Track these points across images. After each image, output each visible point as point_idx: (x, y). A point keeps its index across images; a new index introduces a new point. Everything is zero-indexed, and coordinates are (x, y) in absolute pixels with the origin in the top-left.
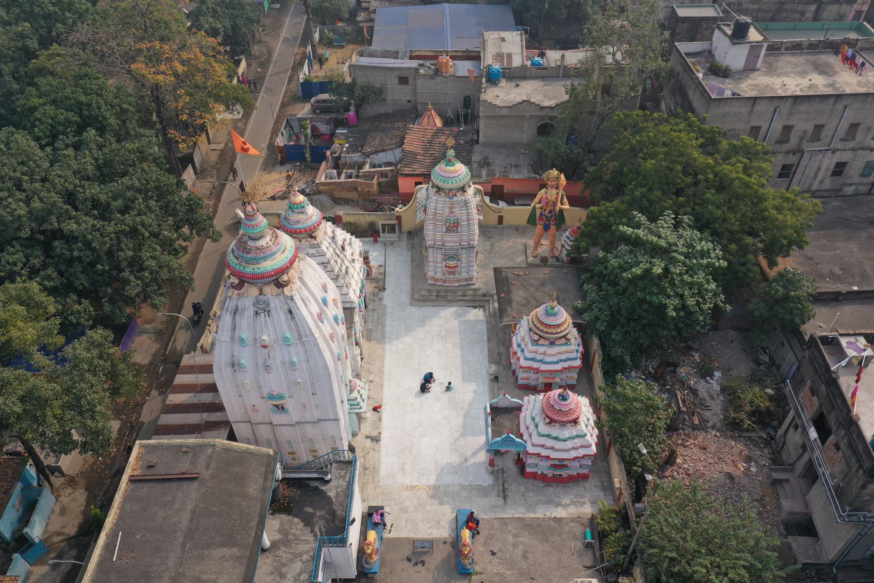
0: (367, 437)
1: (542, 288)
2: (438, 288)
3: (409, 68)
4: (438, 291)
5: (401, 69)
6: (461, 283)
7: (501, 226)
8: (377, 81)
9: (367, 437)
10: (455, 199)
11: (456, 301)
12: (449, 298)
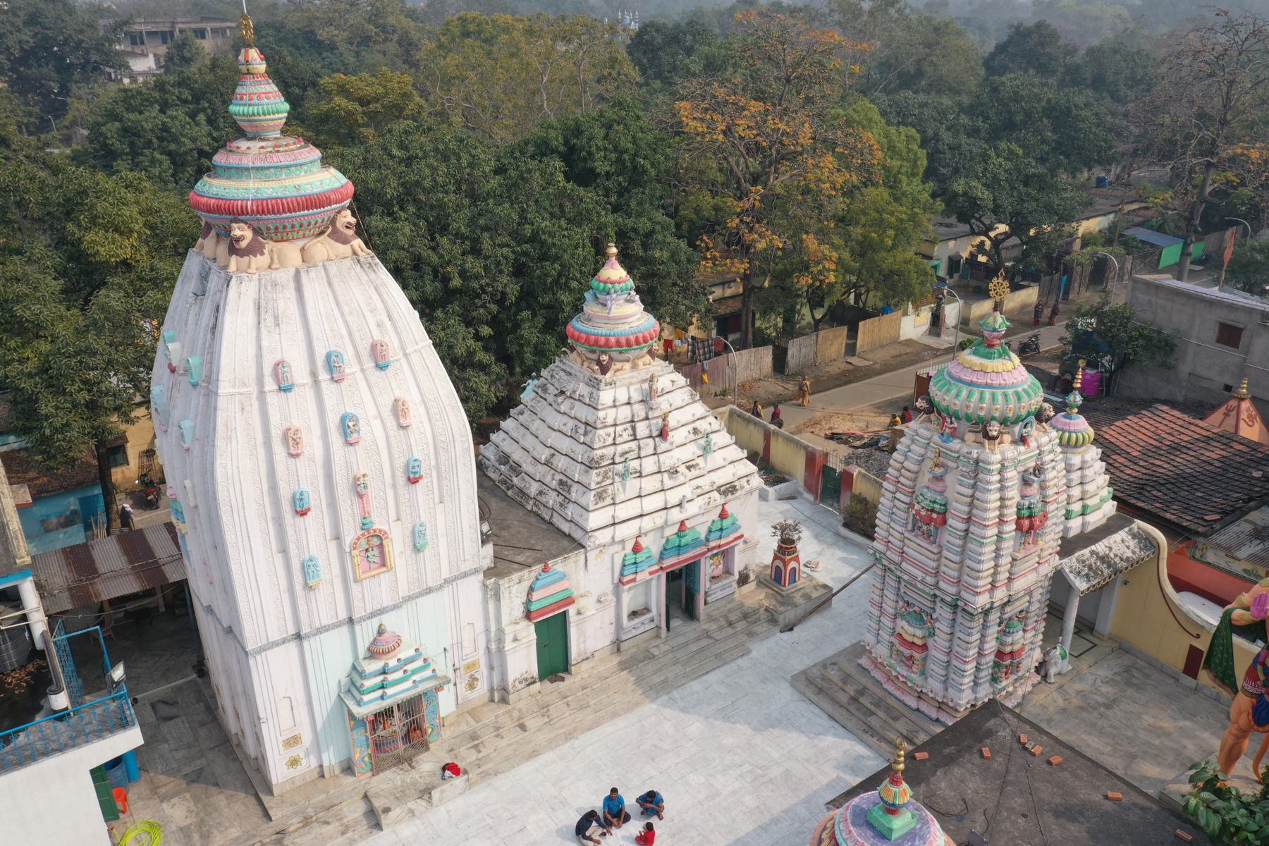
0: (366, 797)
1: (1049, 819)
2: (869, 684)
3: (1250, 311)
4: (862, 691)
5: (1232, 307)
6: (924, 707)
7: (1188, 680)
8: (1169, 319)
9: (366, 797)
10: (955, 444)
11: (882, 738)
12: (873, 721)
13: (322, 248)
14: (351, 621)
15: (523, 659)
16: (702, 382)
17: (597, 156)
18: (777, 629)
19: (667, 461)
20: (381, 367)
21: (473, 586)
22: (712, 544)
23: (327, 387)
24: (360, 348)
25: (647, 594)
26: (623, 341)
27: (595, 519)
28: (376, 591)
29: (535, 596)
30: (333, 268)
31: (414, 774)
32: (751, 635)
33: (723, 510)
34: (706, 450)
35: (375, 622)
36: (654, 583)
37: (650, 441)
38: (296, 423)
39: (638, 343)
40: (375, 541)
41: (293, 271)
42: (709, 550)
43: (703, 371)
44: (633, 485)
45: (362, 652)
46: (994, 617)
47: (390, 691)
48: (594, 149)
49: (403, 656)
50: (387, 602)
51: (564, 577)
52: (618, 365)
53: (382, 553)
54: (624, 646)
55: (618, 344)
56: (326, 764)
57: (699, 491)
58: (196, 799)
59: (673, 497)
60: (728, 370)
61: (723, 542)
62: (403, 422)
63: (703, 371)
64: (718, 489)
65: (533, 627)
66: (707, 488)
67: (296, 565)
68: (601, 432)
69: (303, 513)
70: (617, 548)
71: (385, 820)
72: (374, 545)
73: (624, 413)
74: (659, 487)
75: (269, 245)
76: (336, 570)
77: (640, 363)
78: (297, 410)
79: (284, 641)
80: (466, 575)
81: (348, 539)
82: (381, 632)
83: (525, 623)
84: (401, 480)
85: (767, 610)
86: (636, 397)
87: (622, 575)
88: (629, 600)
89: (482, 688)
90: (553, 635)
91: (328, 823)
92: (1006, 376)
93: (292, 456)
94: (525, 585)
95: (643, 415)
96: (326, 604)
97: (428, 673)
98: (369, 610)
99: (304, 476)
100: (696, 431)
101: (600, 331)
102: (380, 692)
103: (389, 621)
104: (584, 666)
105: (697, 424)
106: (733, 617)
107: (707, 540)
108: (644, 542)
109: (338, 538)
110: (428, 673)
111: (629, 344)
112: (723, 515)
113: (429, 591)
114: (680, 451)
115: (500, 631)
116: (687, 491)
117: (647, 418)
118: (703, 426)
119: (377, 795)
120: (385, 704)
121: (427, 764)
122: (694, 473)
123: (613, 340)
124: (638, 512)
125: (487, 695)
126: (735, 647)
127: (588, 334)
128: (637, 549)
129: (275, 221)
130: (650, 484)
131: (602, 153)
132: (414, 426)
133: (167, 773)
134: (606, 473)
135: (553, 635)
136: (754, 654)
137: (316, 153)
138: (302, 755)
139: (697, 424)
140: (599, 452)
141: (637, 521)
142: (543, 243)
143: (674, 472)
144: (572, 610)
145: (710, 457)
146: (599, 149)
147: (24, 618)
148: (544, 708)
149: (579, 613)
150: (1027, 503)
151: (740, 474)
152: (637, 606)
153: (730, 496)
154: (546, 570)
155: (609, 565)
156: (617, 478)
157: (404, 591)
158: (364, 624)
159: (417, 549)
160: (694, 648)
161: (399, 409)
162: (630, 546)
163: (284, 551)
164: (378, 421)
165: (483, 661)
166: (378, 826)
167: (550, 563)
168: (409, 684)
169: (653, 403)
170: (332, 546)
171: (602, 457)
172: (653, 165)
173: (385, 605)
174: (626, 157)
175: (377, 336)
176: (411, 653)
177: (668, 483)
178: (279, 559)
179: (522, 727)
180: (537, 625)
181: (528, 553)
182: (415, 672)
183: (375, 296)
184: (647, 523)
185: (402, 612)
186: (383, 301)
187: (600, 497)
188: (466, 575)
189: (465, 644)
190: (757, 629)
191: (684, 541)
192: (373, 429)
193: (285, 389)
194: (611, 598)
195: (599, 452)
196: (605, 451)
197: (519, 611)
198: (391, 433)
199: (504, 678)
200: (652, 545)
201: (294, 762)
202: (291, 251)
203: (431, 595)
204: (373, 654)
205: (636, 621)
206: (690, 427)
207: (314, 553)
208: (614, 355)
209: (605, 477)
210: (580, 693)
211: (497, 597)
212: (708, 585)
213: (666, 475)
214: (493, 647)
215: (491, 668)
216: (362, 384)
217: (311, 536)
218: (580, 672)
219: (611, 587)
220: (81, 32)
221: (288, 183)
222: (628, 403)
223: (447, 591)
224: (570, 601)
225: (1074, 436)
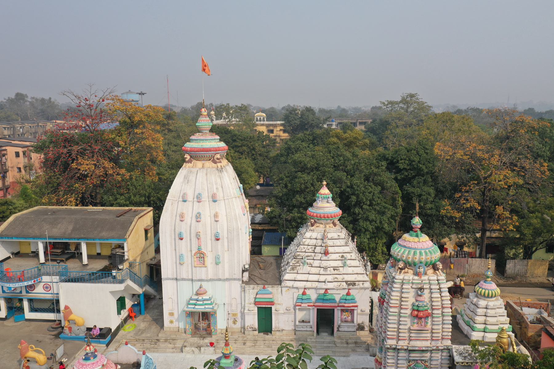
13: (209, 164)
14: (192, 280)
15: (252, 320)
16: (450, 268)
17: (400, 162)
18: (368, 354)
19: (324, 264)
20: (215, 201)
21: (237, 285)
22: (340, 305)
23: (196, 204)
26: (319, 215)
27: (287, 277)
28: (201, 273)
29: (258, 296)
30: (209, 170)
31: (202, 341)
32: (354, 351)
33: (348, 292)
34: (344, 265)
35: (199, 283)
36: (311, 311)
37: (320, 255)
38: (184, 211)
39: (328, 217)
40: (202, 256)
41: (197, 169)
42: (338, 306)
43: (451, 263)
44: (307, 269)
45: (194, 293)
46: (402, 354)
47: (197, 307)
48: (399, 159)
49: (204, 297)
50: (204, 277)
51: (271, 293)
52: (318, 225)
54: (297, 333)
55: (317, 216)
57: (336, 280)
58: (150, 325)
59: (322, 278)
60: (467, 266)
61: (346, 305)
62: (216, 220)
63: (451, 263)
64: (346, 282)
65: (256, 308)
66: (340, 280)
68: (302, 246)
69: (182, 239)
70: (296, 290)
71: (185, 350)
72: (201, 256)
73: (314, 242)
74: (318, 272)
75: (194, 161)
76: (190, 261)
77: (328, 226)
78: (189, 210)
79: (173, 279)
80: (235, 279)
81: (193, 252)
82: (200, 288)
83: (254, 305)
84: (213, 238)
85: (368, 344)
86: (319, 237)
88: (300, 315)
89: (238, 325)
90: (265, 315)
91: (170, 344)
92: (413, 244)
93: (182, 221)
94: (255, 291)
95: (320, 244)
97: (211, 307)
98: (198, 278)
99: (184, 228)
100: (342, 256)
101: (313, 211)
102: (193, 306)
103: (204, 284)
104: (278, 333)
105: (344, 255)
106: (350, 341)
107: (340, 303)
108: (307, 291)
110: (211, 307)
111: (320, 217)
112: (348, 294)
113: (220, 280)
114: (333, 261)
115: (244, 306)
116: (330, 278)
117: (321, 246)
118: (348, 256)
119: (187, 342)
120: (193, 310)
121: (208, 341)
122: (336, 272)
123: (315, 214)
124: (306, 279)
126: (344, 352)
127: (317, 214)
128: (304, 293)
129: (198, 155)
130: (314, 270)
131: (403, 161)
132: (220, 221)
133: (150, 316)
134: (298, 261)
135: (265, 315)
136: (350, 358)
137: (218, 137)
138: (174, 321)
139: (344, 255)
140: (298, 253)
141: (305, 282)
142: (353, 188)
143: (325, 268)
145: (345, 268)
146: (401, 159)
147: (124, 253)
148: (256, 341)
150: (417, 304)
151: (359, 279)
153: (351, 287)
154: (264, 288)
156: (301, 264)
159: (217, 264)
160: (325, 345)
161: (216, 216)
162: (301, 291)
166: (182, 351)
167: (266, 286)
168: (203, 307)
169: (325, 241)
170: (189, 253)
171: (299, 255)
172: (426, 168)
174: (414, 163)
175: (215, 191)
176: (208, 298)
177: (322, 272)
178: (174, 252)
179: (244, 344)
180: (258, 308)
181: (263, 282)
182: (206, 304)
183: (219, 180)
184: (308, 285)
185: (210, 283)
187: (293, 269)
188: (235, 279)
189: (233, 305)
190: (358, 350)
191: (326, 298)
192: (207, 218)
193: (185, 201)
194: (292, 310)
195: (298, 253)
196: (301, 253)
197: (252, 301)
200: (313, 295)
201: (171, 322)
202: (199, 164)
203: (220, 282)
204: (197, 294)
205: (302, 324)
206: (341, 255)
207: (184, 252)
208: (316, 220)
209: (298, 262)
210: (271, 342)
212: (339, 322)
213: (322, 269)
216: (208, 205)
217: (184, 246)
218: (276, 335)
220: (313, 120)
221: (200, 144)
222: (316, 239)
223: (227, 283)
224: (272, 303)
225: (487, 291)
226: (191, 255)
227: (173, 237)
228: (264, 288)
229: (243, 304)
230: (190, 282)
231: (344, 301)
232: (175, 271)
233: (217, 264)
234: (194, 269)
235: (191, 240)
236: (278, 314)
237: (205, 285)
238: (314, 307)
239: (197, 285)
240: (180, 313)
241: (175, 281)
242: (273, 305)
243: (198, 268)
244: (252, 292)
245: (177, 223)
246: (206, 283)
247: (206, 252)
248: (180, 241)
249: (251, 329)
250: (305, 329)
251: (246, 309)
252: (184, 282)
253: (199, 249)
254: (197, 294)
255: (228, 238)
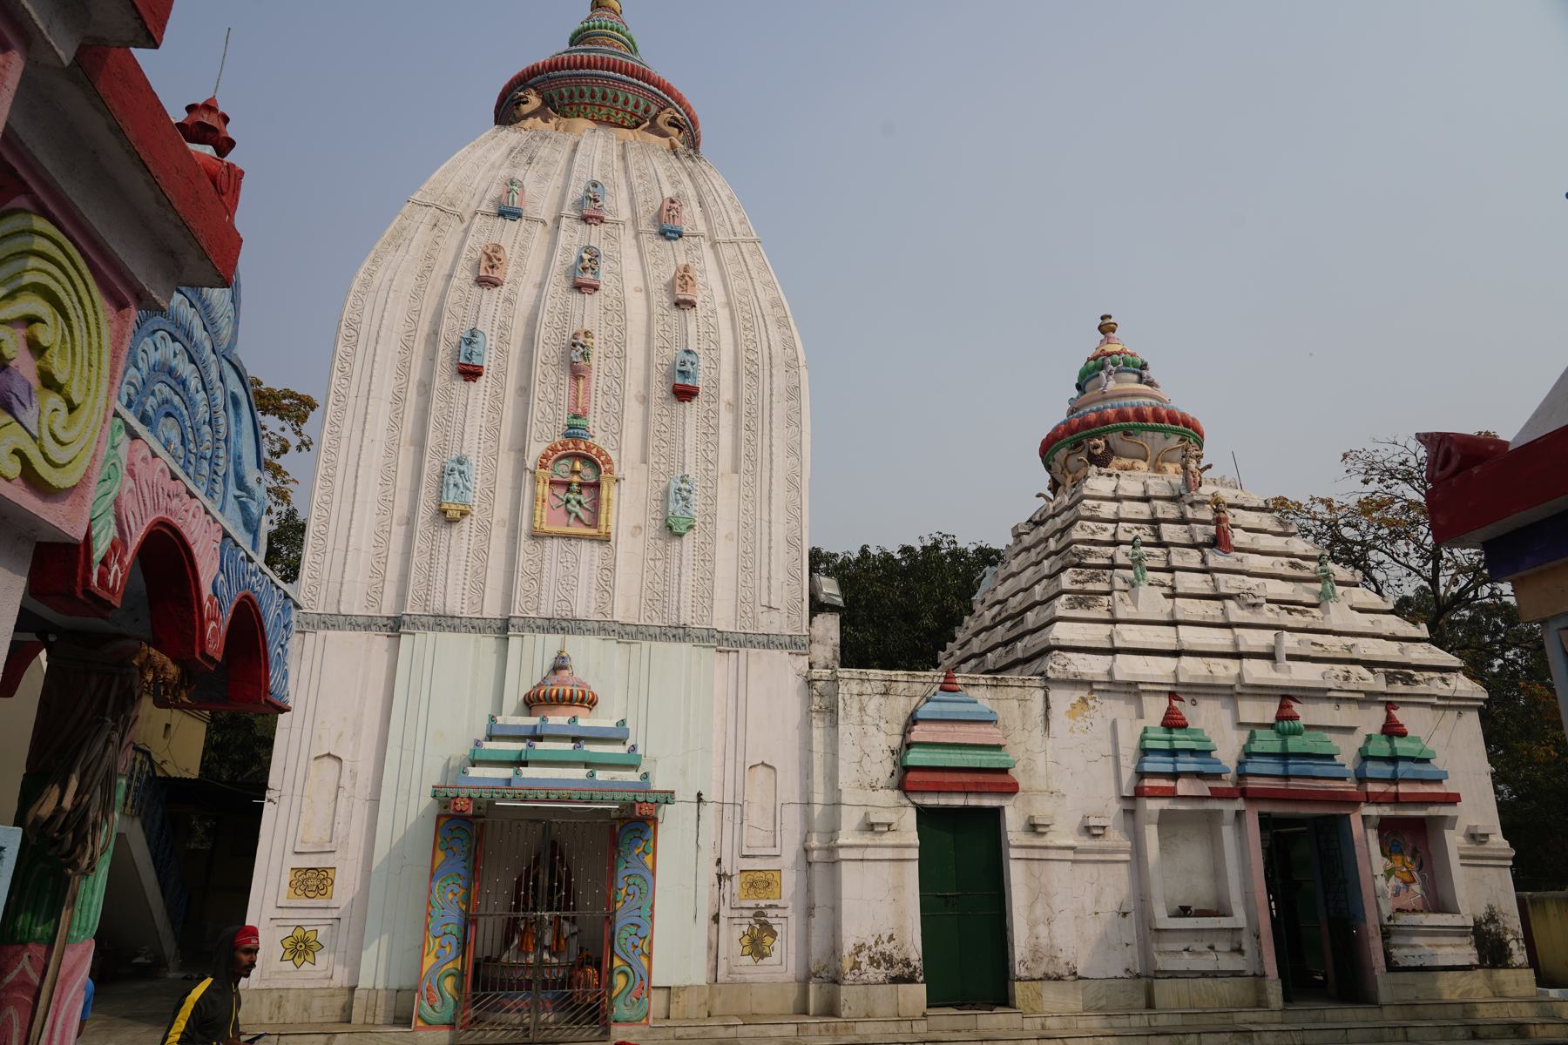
15: (883, 903)
21: (777, 679)
24: (641, 210)
25: (1217, 873)
28: (569, 577)
36: (1228, 832)
40: (589, 475)
47: (527, 772)
50: (584, 606)
52: (1126, 462)
53: (596, 503)
56: (365, 982)
65: (911, 815)
67: (431, 466)
69: (470, 373)
72: (579, 472)
76: (502, 510)
79: (368, 624)
80: (770, 642)
81: (535, 450)
82: (556, 669)
83: (893, 796)
84: (660, 390)
87: (1141, 775)
89: (784, 961)
90: (964, 853)
94: (900, 707)
96: (463, 573)
97: (632, 776)
98: (546, 611)
104: (1050, 993)
108: (1185, 708)
109: (521, 450)
110: (632, 776)
113: (679, 633)
125: (793, 993)
128: (1172, 722)
132: (701, 310)
135: (964, 853)
144: (1013, 818)
149: (1033, 828)
152: (1199, 891)
155: (1107, 747)
157: (624, 610)
158: (528, 636)
159: (671, 531)
162: (1156, 709)
163: (420, 444)
164: (642, 295)
165: (790, 882)
173: (580, 613)
180: (924, 814)
186: (697, 187)
188: (770, 642)
189: (755, 815)
194: (1116, 838)
197: (882, 768)
198: (657, 310)
199: (835, 951)
201: (301, 948)
203: (685, 647)
211: (831, 712)
214: (815, 842)
215: (809, 911)
219: (1116, 807)
226: (521, 467)
227: (416, 375)
228: (948, 687)
229: (819, 797)
230: (489, 642)
231: (1385, 770)
232: (393, 573)
233: (671, 531)
234: (524, 544)
235: (525, 390)
236: (1039, 858)
237: (592, 661)
238: (1239, 804)
239: (530, 660)
240: (395, 841)
241: (380, 641)
242: (1011, 790)
243: (552, 546)
244: (878, 707)
245: (453, 296)
246: (593, 640)
247: (613, 456)
248: (460, 384)
249: (880, 974)
250: (1206, 963)
251: (850, 820)
252: (446, 638)
253: (574, 432)
254: (531, 703)
255: (734, 406)
